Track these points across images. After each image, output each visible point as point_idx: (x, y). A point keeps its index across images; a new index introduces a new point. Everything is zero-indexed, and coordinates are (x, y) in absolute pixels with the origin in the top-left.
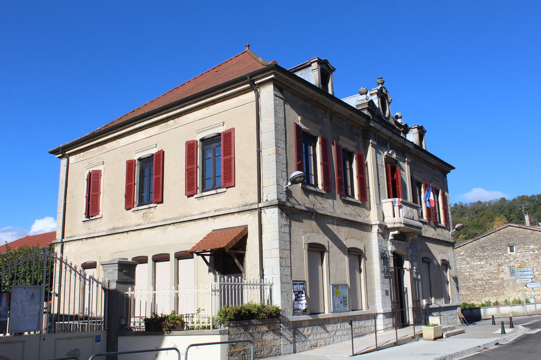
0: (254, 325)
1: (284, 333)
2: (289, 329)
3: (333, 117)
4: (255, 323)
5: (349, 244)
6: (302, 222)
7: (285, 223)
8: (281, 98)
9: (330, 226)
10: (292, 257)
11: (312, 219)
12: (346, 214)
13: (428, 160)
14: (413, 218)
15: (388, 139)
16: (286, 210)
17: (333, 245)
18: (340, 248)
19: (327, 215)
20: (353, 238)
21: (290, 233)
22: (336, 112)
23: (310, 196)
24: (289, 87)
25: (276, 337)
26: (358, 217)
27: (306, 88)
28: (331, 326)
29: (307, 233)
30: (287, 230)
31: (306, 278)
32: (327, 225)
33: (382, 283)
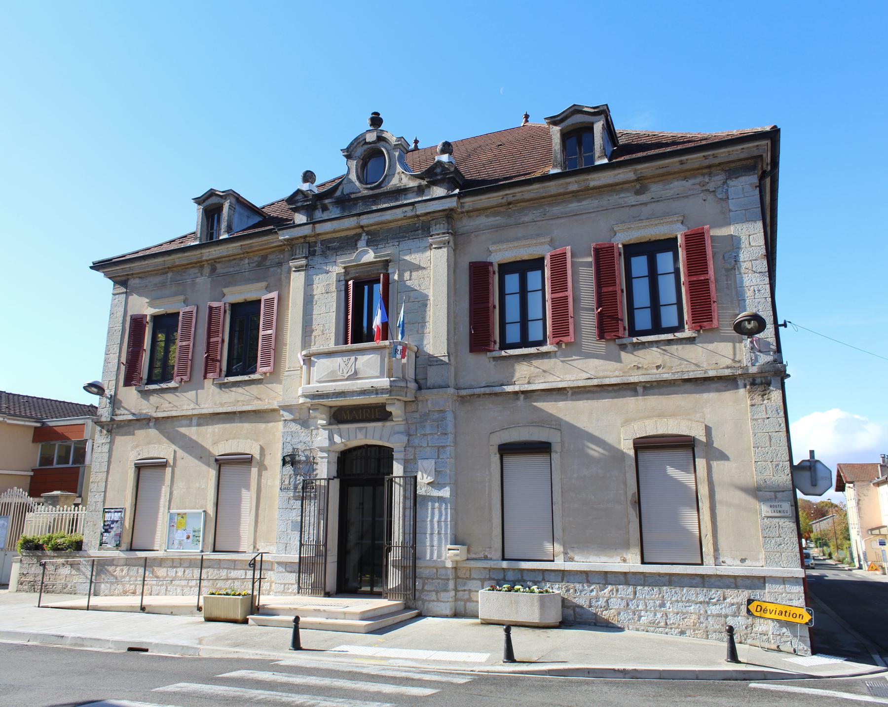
1: (83, 569)
3: (218, 266)
5: (219, 450)
6: (134, 434)
9: (183, 430)
10: (110, 479)
12: (222, 405)
14: (356, 373)
15: (359, 231)
16: (108, 425)
17: (186, 455)
18: (200, 458)
19: (172, 417)
20: (234, 438)
21: (110, 451)
23: (151, 398)
25: (74, 572)
26: (256, 402)
27: (156, 260)
28: (165, 570)
32: (179, 429)
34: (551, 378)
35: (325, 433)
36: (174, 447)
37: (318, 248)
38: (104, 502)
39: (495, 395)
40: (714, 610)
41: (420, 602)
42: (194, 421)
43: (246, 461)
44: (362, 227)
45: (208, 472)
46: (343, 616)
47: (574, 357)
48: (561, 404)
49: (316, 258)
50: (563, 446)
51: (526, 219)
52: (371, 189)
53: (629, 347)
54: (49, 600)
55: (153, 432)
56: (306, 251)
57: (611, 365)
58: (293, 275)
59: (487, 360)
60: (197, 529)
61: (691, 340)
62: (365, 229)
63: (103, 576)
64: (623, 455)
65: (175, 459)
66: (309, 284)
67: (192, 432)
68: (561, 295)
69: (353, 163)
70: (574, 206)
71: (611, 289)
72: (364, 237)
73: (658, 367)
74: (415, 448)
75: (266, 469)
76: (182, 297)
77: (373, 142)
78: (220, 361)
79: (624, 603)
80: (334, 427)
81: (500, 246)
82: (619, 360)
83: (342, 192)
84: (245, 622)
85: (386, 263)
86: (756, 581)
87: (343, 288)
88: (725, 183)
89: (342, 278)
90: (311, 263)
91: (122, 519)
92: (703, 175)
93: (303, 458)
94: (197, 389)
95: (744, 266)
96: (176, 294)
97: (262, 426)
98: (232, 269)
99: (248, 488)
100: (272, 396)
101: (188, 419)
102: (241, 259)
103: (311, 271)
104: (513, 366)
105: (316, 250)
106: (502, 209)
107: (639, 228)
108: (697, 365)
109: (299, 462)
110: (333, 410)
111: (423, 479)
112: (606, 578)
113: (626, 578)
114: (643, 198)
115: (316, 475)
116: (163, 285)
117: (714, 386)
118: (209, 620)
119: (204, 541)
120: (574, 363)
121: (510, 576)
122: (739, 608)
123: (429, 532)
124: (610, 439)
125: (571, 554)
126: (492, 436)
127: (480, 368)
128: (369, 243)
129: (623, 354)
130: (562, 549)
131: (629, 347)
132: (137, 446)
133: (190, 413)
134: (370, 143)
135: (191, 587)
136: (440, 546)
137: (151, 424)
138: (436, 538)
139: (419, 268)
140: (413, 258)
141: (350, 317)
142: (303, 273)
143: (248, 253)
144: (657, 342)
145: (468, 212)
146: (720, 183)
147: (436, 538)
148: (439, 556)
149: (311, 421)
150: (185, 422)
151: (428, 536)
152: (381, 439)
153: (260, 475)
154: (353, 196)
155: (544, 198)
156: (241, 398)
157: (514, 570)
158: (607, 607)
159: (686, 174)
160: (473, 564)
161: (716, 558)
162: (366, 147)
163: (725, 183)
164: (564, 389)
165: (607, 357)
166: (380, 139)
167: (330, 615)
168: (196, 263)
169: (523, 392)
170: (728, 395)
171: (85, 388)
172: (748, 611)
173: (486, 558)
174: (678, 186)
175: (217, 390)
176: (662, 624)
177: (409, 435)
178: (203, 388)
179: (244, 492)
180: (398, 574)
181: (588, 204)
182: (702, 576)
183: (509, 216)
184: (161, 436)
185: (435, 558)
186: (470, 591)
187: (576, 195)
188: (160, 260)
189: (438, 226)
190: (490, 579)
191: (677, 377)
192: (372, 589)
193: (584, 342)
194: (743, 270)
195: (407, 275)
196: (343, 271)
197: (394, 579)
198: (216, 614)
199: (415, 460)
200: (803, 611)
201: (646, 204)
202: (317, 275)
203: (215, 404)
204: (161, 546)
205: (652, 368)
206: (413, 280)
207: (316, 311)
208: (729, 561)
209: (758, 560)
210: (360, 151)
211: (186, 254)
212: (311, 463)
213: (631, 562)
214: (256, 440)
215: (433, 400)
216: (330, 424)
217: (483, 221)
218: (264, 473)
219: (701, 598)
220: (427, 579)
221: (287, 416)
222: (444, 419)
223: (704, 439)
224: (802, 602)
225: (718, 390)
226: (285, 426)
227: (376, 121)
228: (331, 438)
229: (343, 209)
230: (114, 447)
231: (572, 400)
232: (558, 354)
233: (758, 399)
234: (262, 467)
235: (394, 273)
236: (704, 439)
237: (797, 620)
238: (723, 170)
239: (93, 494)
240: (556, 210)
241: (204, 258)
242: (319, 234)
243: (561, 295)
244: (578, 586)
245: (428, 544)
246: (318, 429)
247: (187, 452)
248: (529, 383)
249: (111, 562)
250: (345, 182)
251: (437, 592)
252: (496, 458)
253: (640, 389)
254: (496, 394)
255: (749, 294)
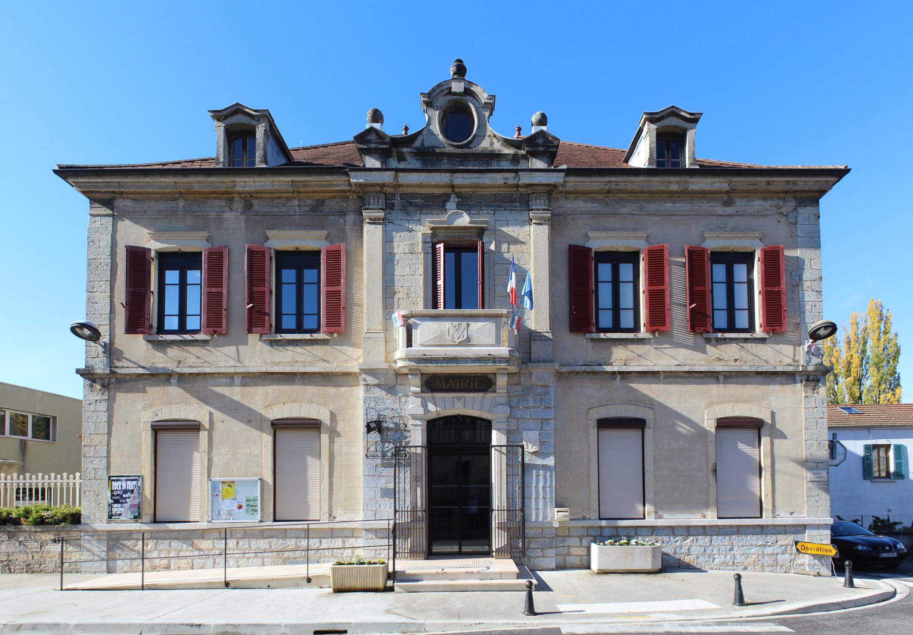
0: (25, 531)
1: (87, 545)
2: (99, 540)
3: (255, 202)
4: (27, 529)
7: (98, 398)
8: (107, 215)
9: (220, 390)
10: (113, 442)
11: (170, 384)
12: (275, 364)
13: (674, 188)
17: (226, 418)
18: (249, 422)
19: (205, 374)
20: (294, 401)
22: (257, 192)
23: (169, 350)
24: (122, 193)
27: (163, 179)
28: (210, 542)
29: (141, 410)
30: (103, 406)
31: (146, 471)
33: (370, 476)
34: (645, 362)
35: (418, 401)
36: (208, 408)
37: (397, 201)
38: (108, 468)
39: (595, 373)
40: (769, 550)
41: (526, 559)
42: (237, 380)
43: (313, 425)
44: (453, 187)
45: (262, 437)
46: (499, 576)
47: (666, 346)
48: (654, 386)
49: (395, 213)
50: (655, 423)
51: (624, 210)
52: (458, 147)
53: (713, 341)
54: (71, 581)
55: (174, 390)
56: (382, 202)
57: (698, 355)
58: (366, 228)
59: (585, 341)
60: (251, 498)
61: (762, 341)
62: (456, 190)
63: (118, 552)
64: (705, 432)
65: (211, 421)
66: (387, 241)
67: (236, 393)
68: (658, 288)
69: (436, 115)
70: (668, 206)
71: (702, 288)
72: (454, 199)
73: (736, 360)
74: (518, 419)
75: (339, 435)
76: (205, 234)
77: (460, 94)
78: (269, 315)
79: (703, 549)
80: (429, 395)
81: (599, 234)
82: (705, 352)
83: (422, 144)
84: (391, 589)
85: (481, 232)
86: (799, 528)
87: (430, 250)
88: (795, 209)
89: (429, 240)
90: (388, 216)
91: (140, 490)
92: (779, 199)
93: (392, 425)
94: (237, 344)
95: (806, 284)
96: (194, 229)
97: (332, 390)
98: (275, 210)
99: (319, 456)
100: (350, 358)
101: (230, 378)
102: (288, 199)
103: (390, 227)
104: (610, 348)
105: (399, 205)
106: (600, 197)
107: (725, 238)
108: (766, 361)
109: (388, 429)
110: (425, 378)
111: (530, 448)
112: (689, 531)
113: (704, 530)
114: (730, 210)
115: (409, 442)
116: (173, 213)
117: (778, 379)
118: (338, 591)
119: (262, 510)
120: (666, 351)
121: (606, 533)
122: (786, 548)
123: (534, 496)
124: (696, 418)
125: (660, 513)
126: (591, 411)
127: (579, 347)
128: (459, 206)
129: (708, 346)
130: (653, 509)
131: (713, 341)
132: (152, 405)
133: (232, 370)
134: (455, 94)
135: (248, 558)
136: (545, 509)
137: (172, 381)
138: (541, 502)
139: (517, 241)
140: (512, 230)
141: (440, 283)
142: (380, 227)
143: (299, 192)
144: (736, 339)
145: (566, 192)
146: (791, 209)
147: (541, 502)
148: (545, 517)
149: (399, 388)
150: (224, 381)
151: (533, 500)
152: (481, 409)
153: (332, 442)
154: (437, 150)
155: (642, 192)
156: (302, 359)
157: (609, 527)
158: (689, 554)
159: (767, 195)
160: (573, 524)
161: (773, 512)
162: (449, 98)
163: (795, 209)
164: (658, 372)
165: (694, 348)
166: (468, 92)
167: (481, 575)
168: (223, 193)
169: (620, 373)
170: (788, 388)
171: (73, 330)
172: (797, 550)
173: (584, 518)
174: (758, 204)
175: (267, 348)
176: (731, 563)
177: (511, 407)
178: (246, 344)
179: (311, 461)
180: (504, 535)
181: (681, 206)
182: (762, 526)
183: (607, 205)
184: (187, 395)
185: (541, 519)
186: (569, 547)
187: (672, 196)
188: (169, 180)
189: (538, 201)
190: (588, 536)
191: (753, 369)
192: (460, 549)
193: (675, 333)
194: (805, 288)
195: (504, 247)
196: (430, 232)
197: (498, 539)
198: (348, 584)
199: (518, 431)
200: (831, 547)
201: (731, 216)
202: (397, 231)
203: (265, 363)
204: (201, 517)
205: (731, 361)
206: (510, 252)
207: (398, 271)
208: (782, 514)
209: (802, 513)
210: (442, 101)
211: (211, 179)
212: (400, 431)
213: (710, 518)
214: (324, 405)
215: (541, 374)
216: (422, 392)
217: (580, 205)
218: (336, 439)
219: (760, 543)
220: (533, 538)
221: (371, 380)
222: (547, 393)
223: (769, 422)
224: (828, 541)
225: (782, 384)
226: (367, 391)
227: (461, 70)
228: (424, 405)
229: (425, 163)
230: (115, 406)
231: (664, 383)
232: (652, 341)
233: (810, 392)
234: (334, 433)
235: (491, 242)
236: (769, 422)
237: (828, 554)
238: (795, 197)
239: (89, 460)
240: (652, 207)
241: (238, 189)
242: (400, 186)
243: (658, 288)
244: (666, 538)
245: (533, 507)
246: (407, 396)
247: (228, 415)
248: (625, 365)
249: (129, 534)
250: (425, 132)
251: (542, 549)
252: (593, 431)
253: (721, 378)
254: (595, 373)
255: (808, 307)
